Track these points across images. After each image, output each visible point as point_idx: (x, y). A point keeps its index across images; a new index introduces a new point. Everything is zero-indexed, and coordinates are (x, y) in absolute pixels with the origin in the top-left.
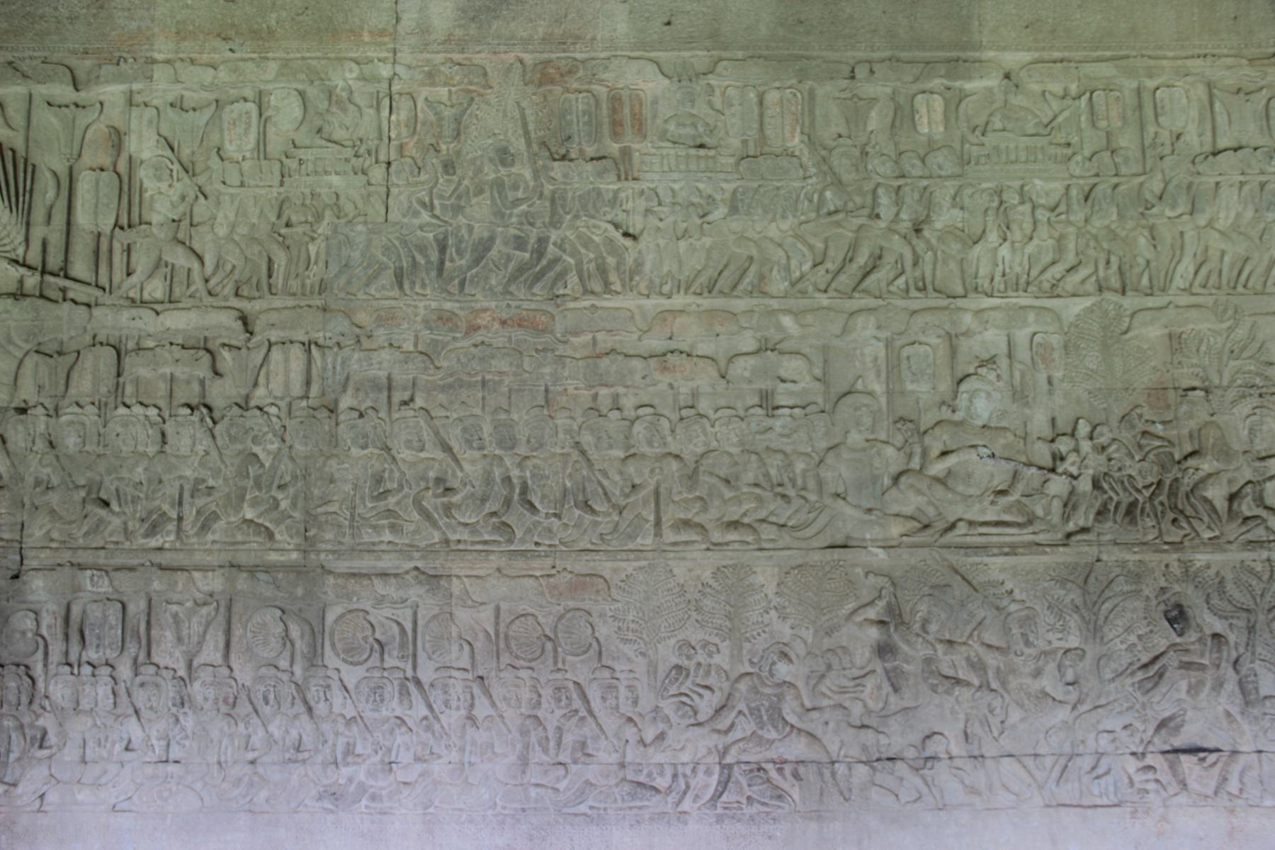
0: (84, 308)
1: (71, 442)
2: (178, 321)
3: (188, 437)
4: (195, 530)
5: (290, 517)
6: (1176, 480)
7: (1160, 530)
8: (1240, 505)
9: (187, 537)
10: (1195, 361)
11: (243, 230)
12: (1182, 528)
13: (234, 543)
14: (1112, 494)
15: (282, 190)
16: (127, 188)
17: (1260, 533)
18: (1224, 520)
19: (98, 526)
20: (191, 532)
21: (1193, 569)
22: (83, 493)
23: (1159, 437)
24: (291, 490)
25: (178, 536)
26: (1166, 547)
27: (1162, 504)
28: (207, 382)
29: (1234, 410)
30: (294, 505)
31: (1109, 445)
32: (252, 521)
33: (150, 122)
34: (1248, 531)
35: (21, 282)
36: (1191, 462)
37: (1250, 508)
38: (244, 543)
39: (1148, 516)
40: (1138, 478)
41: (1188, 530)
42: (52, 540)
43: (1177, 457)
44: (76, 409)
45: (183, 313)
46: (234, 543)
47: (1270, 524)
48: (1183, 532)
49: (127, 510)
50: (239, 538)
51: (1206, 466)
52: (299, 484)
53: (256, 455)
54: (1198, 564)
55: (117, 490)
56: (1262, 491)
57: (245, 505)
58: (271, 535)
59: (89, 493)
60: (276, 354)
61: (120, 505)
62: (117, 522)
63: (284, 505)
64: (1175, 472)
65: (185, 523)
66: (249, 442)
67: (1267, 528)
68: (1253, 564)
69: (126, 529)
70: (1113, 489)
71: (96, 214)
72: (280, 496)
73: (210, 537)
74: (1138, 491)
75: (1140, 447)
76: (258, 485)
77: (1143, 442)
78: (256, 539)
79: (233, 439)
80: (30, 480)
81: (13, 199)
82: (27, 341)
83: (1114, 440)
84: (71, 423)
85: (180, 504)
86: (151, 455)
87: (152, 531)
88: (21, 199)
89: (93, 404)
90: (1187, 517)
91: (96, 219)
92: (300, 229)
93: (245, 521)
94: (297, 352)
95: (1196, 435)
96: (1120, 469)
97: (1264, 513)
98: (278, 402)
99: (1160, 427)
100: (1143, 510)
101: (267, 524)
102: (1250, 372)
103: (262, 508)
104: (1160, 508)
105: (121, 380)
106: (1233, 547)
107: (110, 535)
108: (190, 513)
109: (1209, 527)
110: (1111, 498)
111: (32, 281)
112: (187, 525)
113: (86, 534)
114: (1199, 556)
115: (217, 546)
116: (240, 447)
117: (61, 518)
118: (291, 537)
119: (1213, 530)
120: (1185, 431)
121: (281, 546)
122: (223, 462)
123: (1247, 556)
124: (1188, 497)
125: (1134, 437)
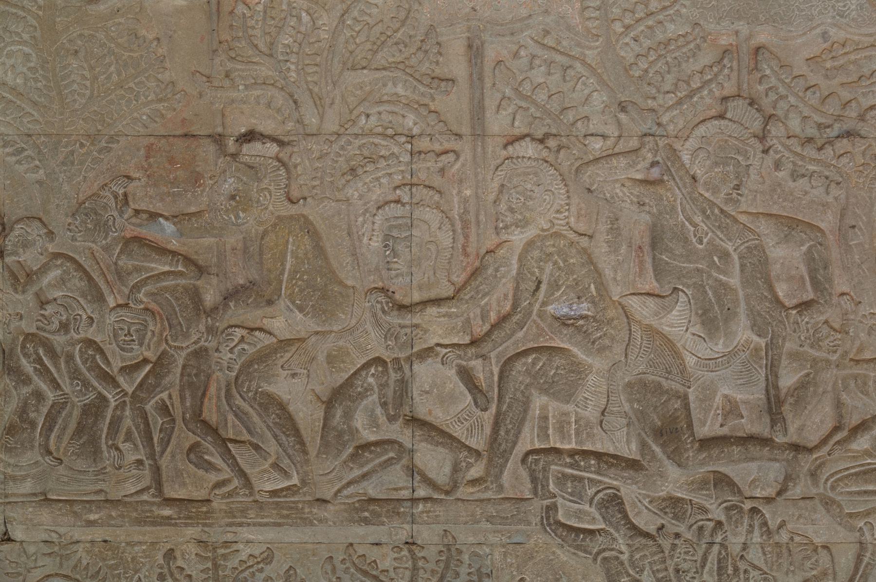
6: (200, 354)
7: (157, 470)
8: (348, 416)
10: (265, 71)
12: (210, 467)
14: (44, 387)
17: (393, 480)
18: (313, 452)
21: (233, 562)
23: (163, 251)
26: (167, 512)
27: (164, 409)
29: (350, 191)
31: (44, 269)
34: (365, 476)
36: (237, 313)
37: (374, 423)
39: (129, 437)
40: (110, 349)
41: (227, 473)
43: (210, 298)
47: (418, 462)
48: (213, 477)
51: (282, 321)
54: (245, 552)
56: (404, 385)
64: (197, 336)
67: (412, 470)
68: (374, 554)
70: (43, 372)
74: (108, 379)
75: (121, 275)
77: (126, 263)
83: (57, 256)
90: (223, 442)
95: (254, 248)
96: (64, 327)
97: (405, 436)
99: (169, 227)
100: (115, 424)
102: (395, 100)
104: (158, 421)
106: (329, 512)
109: (276, 466)
110: (39, 396)
114: (246, 533)
119: (286, 474)
120: (232, 240)
123: (358, 532)
124: (229, 396)
125: (106, 249)
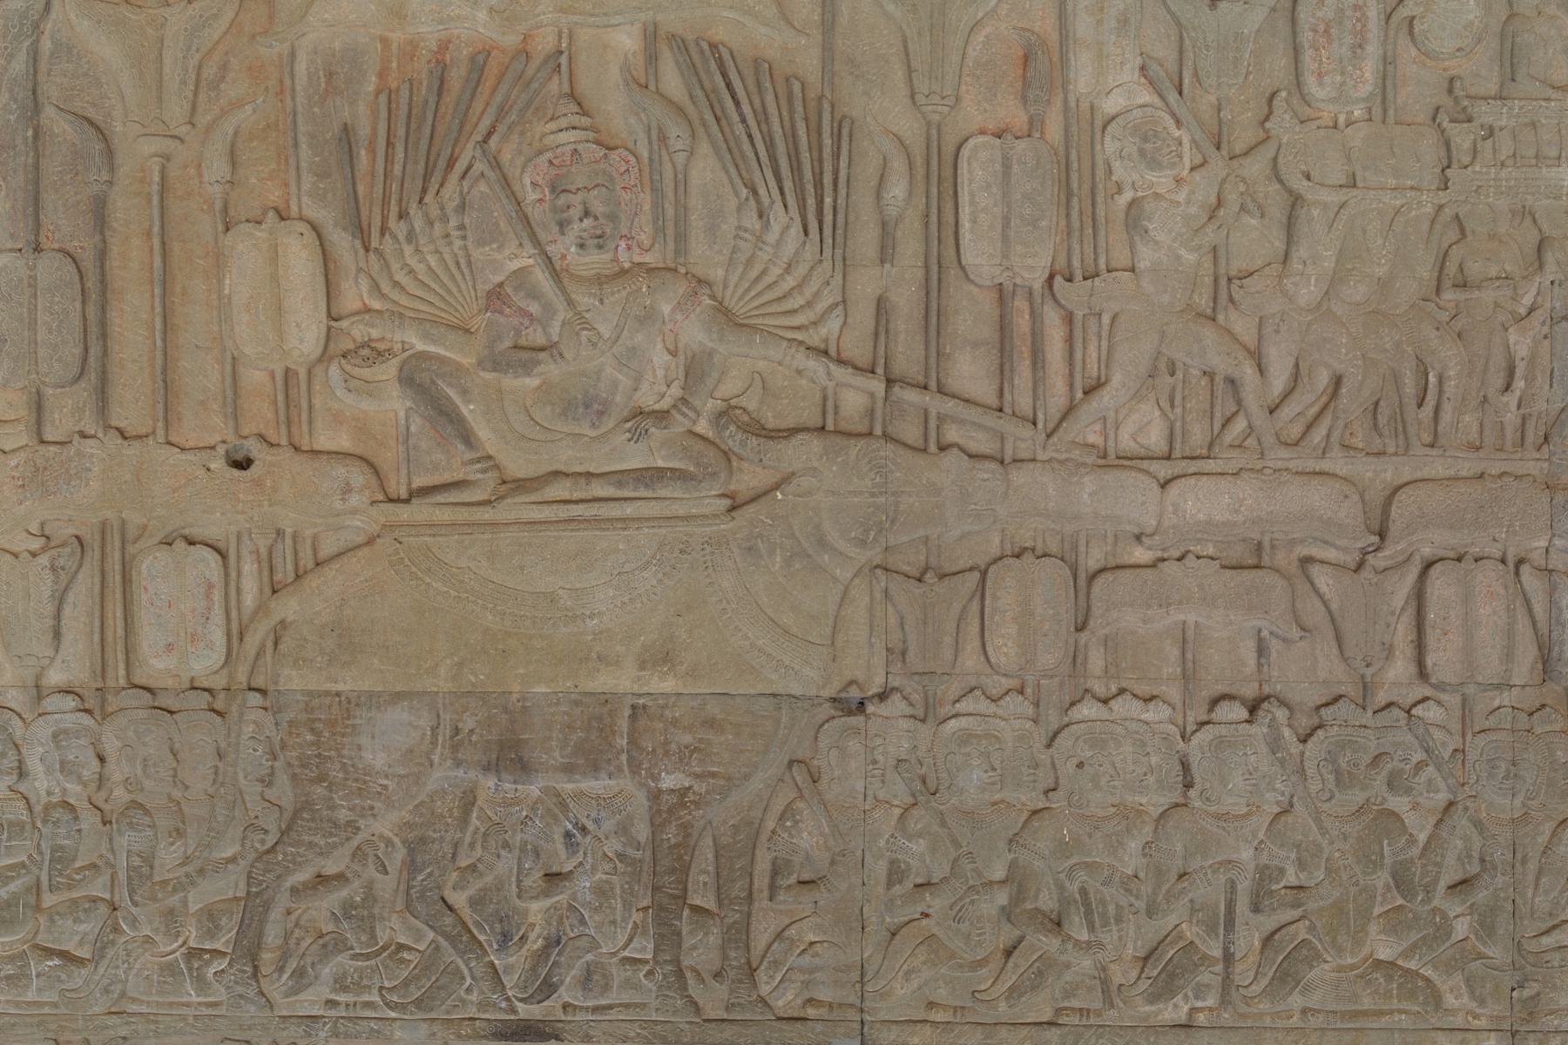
0: (993, 465)
1: (973, 781)
2: (1204, 503)
3: (1245, 772)
4: (1264, 982)
5: (1481, 956)
9: (1247, 1000)
11: (1356, 291)
13: (1356, 1014)
15: (1443, 197)
16: (1076, 187)
19: (1040, 973)
20: (1256, 989)
22: (1002, 898)
24: (1481, 896)
25: (1225, 1000)
28: (1275, 646)
30: (1486, 928)
32: (1393, 964)
33: (1124, 21)
35: (826, 402)
38: (1381, 1013)
42: (931, 1005)
44: (984, 706)
45: (1223, 483)
46: (1356, 1014)
49: (1105, 938)
50: (1367, 1003)
52: (1500, 880)
53: (1393, 814)
55: (1084, 892)
57: (1373, 928)
58: (1436, 999)
59: (1017, 899)
60: (1441, 586)
61: (1091, 928)
62: (1087, 963)
63: (1461, 928)
65: (1239, 968)
66: (1379, 783)
69: (1105, 983)
71: (1005, 239)
72: (1455, 908)
73: (1296, 1001)
76: (1401, 881)
78: (1405, 1005)
79: (1343, 779)
80: (881, 868)
81: (811, 202)
82: (862, 543)
84: (965, 738)
85: (1230, 924)
86: (1155, 812)
87: (1165, 988)
88: (828, 200)
89: (1021, 692)
91: (1005, 256)
92: (1487, 296)
93: (1379, 964)
94: (1489, 579)
98: (1444, 697)
101: (1428, 972)
103: (1415, 936)
105: (1083, 637)
107: (1068, 995)
108: (1248, 940)
111: (855, 396)
112: (1243, 972)
113: (1014, 992)
115: (1316, 1021)
116: (1358, 797)
117: (953, 956)
118: (1482, 1002)
121: (1459, 1021)
122: (1323, 830)
